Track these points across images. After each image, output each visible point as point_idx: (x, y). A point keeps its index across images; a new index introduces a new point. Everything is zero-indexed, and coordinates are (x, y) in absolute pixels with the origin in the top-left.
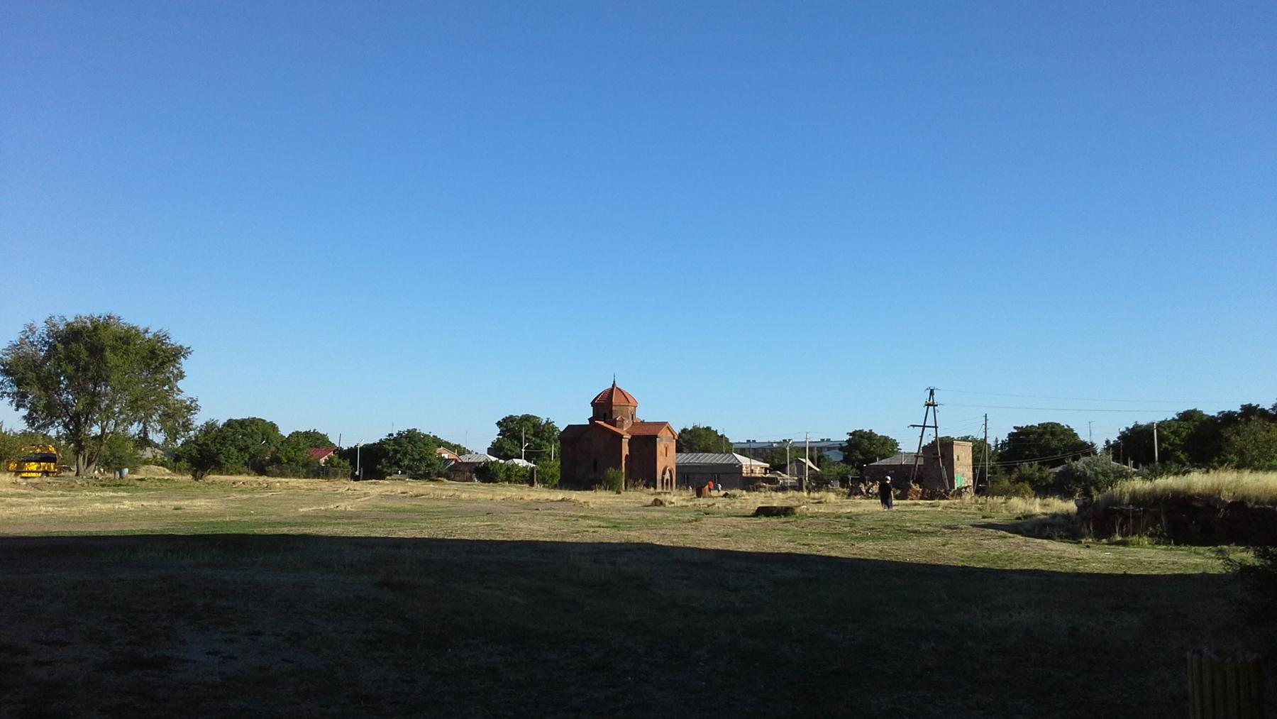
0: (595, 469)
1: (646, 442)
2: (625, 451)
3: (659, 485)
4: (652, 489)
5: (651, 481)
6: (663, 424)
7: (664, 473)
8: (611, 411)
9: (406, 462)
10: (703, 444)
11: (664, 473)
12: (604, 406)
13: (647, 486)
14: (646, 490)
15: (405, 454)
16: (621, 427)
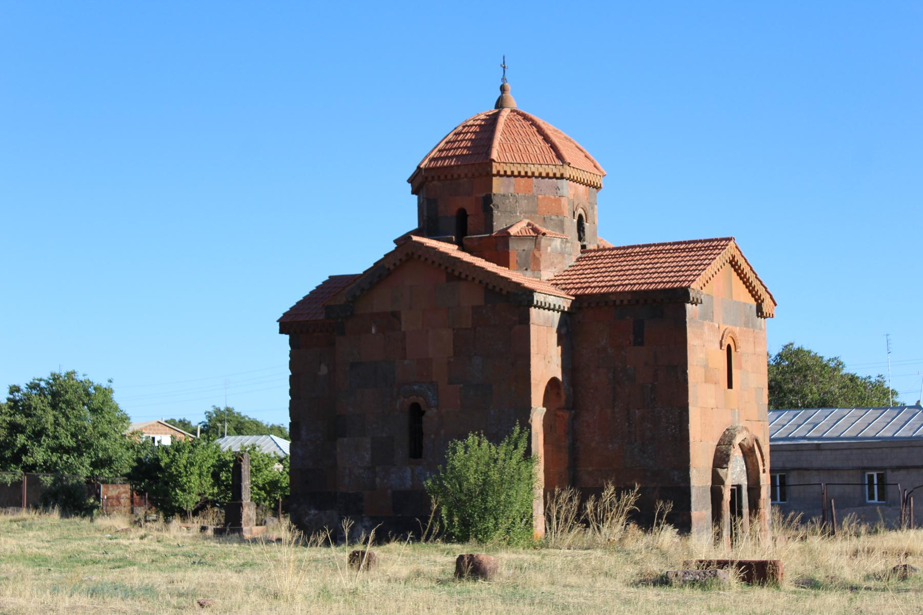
0: (416, 451)
1: (636, 330)
2: (546, 361)
3: (701, 511)
4: (668, 536)
5: (662, 499)
6: (711, 246)
7: (721, 459)
8: (487, 204)
9: (39, 455)
10: (813, 391)
11: (721, 459)
12: (457, 187)
13: (644, 519)
14: (637, 540)
15: (37, 435)
16: (532, 263)
